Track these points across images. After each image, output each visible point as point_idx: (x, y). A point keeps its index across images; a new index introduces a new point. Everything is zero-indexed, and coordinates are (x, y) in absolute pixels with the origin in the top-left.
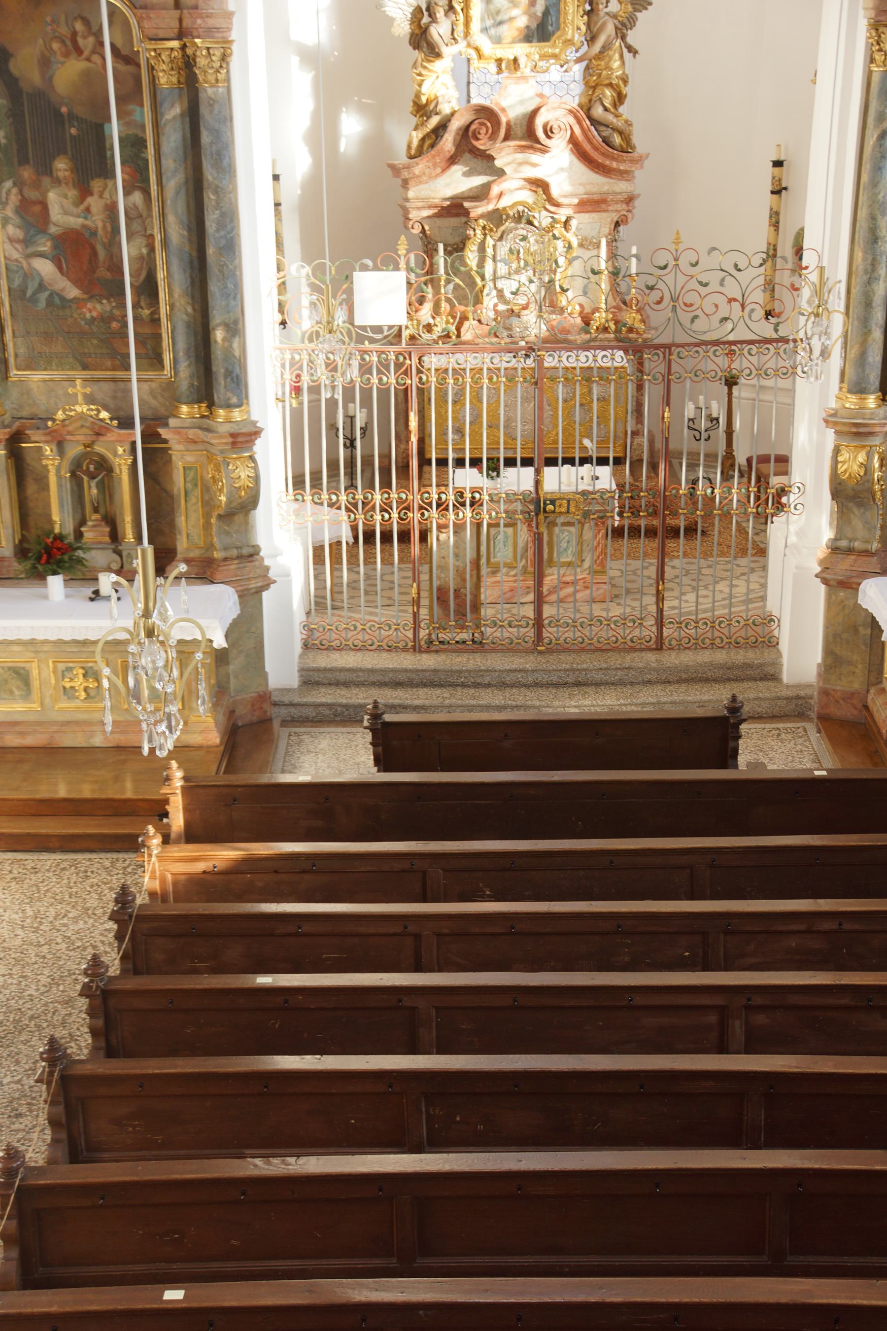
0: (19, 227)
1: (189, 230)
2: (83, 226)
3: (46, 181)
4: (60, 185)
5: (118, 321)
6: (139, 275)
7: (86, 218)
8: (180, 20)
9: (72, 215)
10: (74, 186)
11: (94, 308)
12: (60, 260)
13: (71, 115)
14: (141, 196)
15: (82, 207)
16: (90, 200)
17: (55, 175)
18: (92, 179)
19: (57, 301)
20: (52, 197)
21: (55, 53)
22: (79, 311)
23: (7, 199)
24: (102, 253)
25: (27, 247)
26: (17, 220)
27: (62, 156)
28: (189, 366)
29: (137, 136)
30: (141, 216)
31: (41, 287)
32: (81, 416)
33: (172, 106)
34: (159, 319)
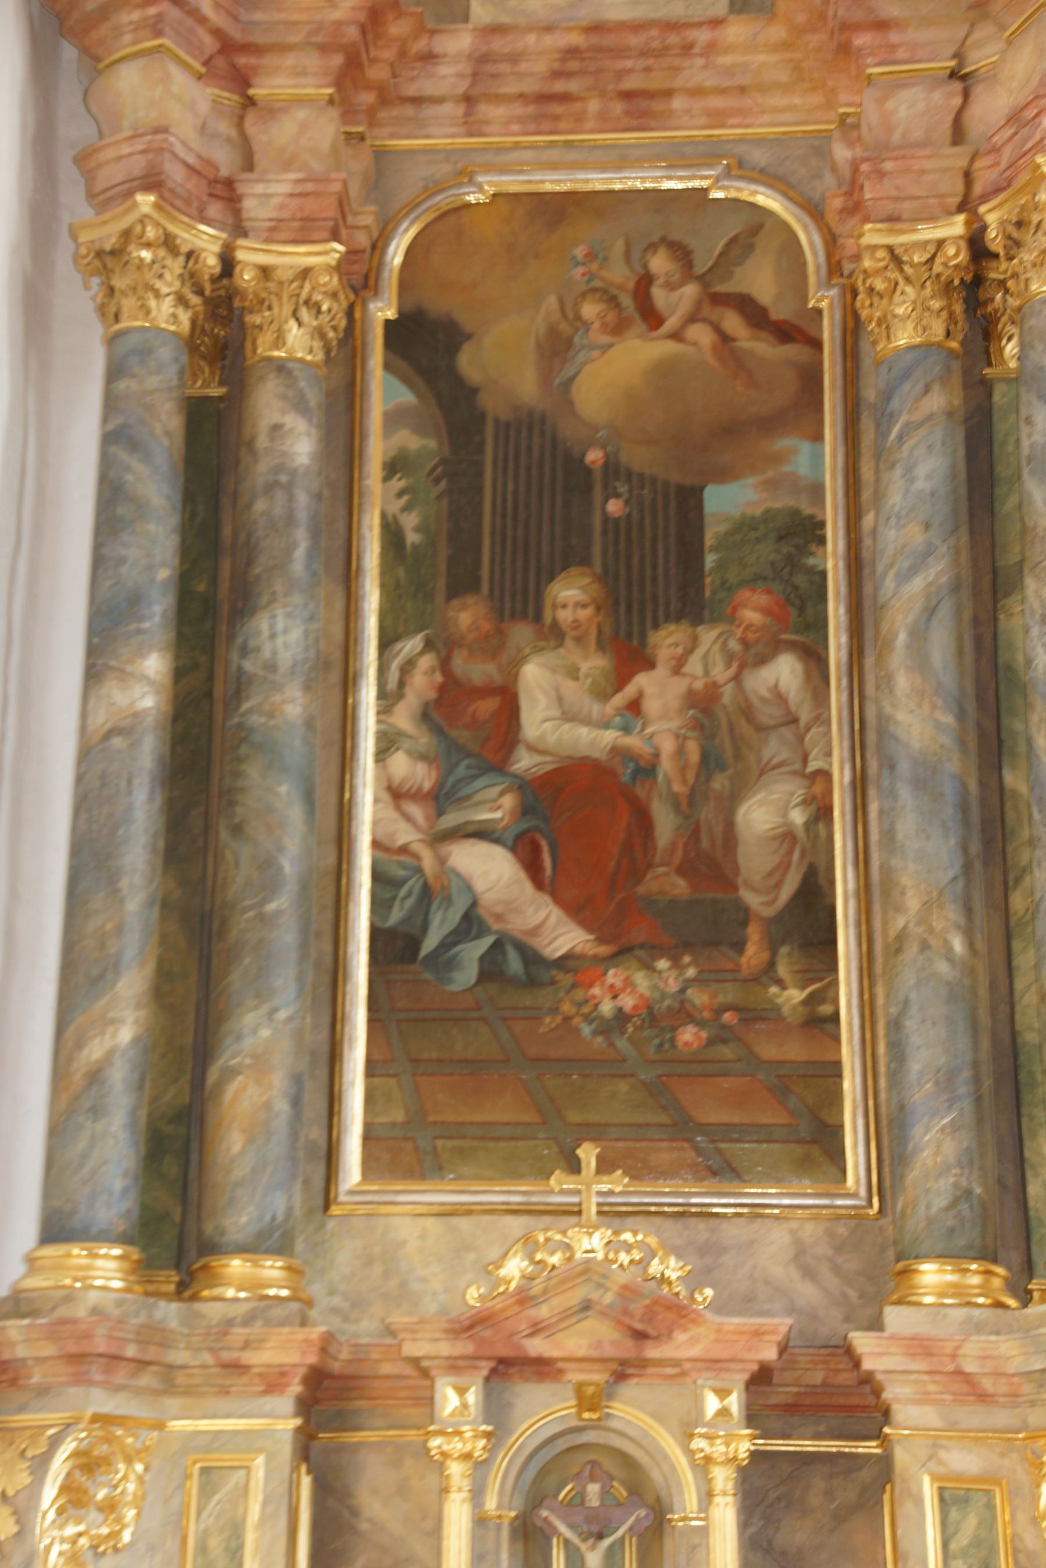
0: (423, 757)
1: (961, 716)
2: (615, 750)
3: (521, 633)
4: (560, 645)
5: (701, 1024)
6: (778, 885)
7: (626, 729)
8: (968, 176)
9: (587, 721)
10: (601, 646)
11: (628, 983)
12: (536, 849)
13: (612, 469)
14: (799, 667)
15: (619, 700)
16: (642, 680)
17: (548, 617)
18: (656, 626)
19: (514, 964)
20: (535, 676)
21: (587, 326)
22: (579, 994)
23: (401, 684)
24: (665, 824)
25: (440, 813)
26: (425, 741)
27: (573, 571)
28: (954, 1127)
29: (795, 513)
30: (795, 721)
31: (471, 923)
32: (587, 1270)
33: (927, 389)
34: (835, 1018)
